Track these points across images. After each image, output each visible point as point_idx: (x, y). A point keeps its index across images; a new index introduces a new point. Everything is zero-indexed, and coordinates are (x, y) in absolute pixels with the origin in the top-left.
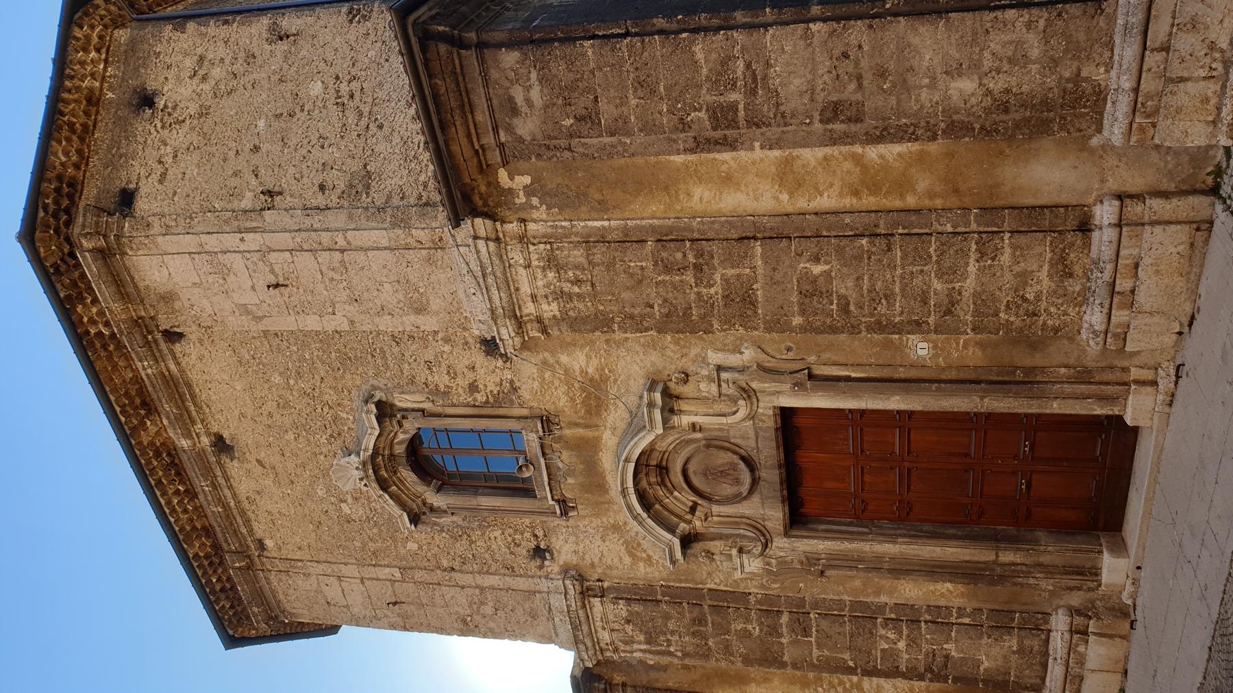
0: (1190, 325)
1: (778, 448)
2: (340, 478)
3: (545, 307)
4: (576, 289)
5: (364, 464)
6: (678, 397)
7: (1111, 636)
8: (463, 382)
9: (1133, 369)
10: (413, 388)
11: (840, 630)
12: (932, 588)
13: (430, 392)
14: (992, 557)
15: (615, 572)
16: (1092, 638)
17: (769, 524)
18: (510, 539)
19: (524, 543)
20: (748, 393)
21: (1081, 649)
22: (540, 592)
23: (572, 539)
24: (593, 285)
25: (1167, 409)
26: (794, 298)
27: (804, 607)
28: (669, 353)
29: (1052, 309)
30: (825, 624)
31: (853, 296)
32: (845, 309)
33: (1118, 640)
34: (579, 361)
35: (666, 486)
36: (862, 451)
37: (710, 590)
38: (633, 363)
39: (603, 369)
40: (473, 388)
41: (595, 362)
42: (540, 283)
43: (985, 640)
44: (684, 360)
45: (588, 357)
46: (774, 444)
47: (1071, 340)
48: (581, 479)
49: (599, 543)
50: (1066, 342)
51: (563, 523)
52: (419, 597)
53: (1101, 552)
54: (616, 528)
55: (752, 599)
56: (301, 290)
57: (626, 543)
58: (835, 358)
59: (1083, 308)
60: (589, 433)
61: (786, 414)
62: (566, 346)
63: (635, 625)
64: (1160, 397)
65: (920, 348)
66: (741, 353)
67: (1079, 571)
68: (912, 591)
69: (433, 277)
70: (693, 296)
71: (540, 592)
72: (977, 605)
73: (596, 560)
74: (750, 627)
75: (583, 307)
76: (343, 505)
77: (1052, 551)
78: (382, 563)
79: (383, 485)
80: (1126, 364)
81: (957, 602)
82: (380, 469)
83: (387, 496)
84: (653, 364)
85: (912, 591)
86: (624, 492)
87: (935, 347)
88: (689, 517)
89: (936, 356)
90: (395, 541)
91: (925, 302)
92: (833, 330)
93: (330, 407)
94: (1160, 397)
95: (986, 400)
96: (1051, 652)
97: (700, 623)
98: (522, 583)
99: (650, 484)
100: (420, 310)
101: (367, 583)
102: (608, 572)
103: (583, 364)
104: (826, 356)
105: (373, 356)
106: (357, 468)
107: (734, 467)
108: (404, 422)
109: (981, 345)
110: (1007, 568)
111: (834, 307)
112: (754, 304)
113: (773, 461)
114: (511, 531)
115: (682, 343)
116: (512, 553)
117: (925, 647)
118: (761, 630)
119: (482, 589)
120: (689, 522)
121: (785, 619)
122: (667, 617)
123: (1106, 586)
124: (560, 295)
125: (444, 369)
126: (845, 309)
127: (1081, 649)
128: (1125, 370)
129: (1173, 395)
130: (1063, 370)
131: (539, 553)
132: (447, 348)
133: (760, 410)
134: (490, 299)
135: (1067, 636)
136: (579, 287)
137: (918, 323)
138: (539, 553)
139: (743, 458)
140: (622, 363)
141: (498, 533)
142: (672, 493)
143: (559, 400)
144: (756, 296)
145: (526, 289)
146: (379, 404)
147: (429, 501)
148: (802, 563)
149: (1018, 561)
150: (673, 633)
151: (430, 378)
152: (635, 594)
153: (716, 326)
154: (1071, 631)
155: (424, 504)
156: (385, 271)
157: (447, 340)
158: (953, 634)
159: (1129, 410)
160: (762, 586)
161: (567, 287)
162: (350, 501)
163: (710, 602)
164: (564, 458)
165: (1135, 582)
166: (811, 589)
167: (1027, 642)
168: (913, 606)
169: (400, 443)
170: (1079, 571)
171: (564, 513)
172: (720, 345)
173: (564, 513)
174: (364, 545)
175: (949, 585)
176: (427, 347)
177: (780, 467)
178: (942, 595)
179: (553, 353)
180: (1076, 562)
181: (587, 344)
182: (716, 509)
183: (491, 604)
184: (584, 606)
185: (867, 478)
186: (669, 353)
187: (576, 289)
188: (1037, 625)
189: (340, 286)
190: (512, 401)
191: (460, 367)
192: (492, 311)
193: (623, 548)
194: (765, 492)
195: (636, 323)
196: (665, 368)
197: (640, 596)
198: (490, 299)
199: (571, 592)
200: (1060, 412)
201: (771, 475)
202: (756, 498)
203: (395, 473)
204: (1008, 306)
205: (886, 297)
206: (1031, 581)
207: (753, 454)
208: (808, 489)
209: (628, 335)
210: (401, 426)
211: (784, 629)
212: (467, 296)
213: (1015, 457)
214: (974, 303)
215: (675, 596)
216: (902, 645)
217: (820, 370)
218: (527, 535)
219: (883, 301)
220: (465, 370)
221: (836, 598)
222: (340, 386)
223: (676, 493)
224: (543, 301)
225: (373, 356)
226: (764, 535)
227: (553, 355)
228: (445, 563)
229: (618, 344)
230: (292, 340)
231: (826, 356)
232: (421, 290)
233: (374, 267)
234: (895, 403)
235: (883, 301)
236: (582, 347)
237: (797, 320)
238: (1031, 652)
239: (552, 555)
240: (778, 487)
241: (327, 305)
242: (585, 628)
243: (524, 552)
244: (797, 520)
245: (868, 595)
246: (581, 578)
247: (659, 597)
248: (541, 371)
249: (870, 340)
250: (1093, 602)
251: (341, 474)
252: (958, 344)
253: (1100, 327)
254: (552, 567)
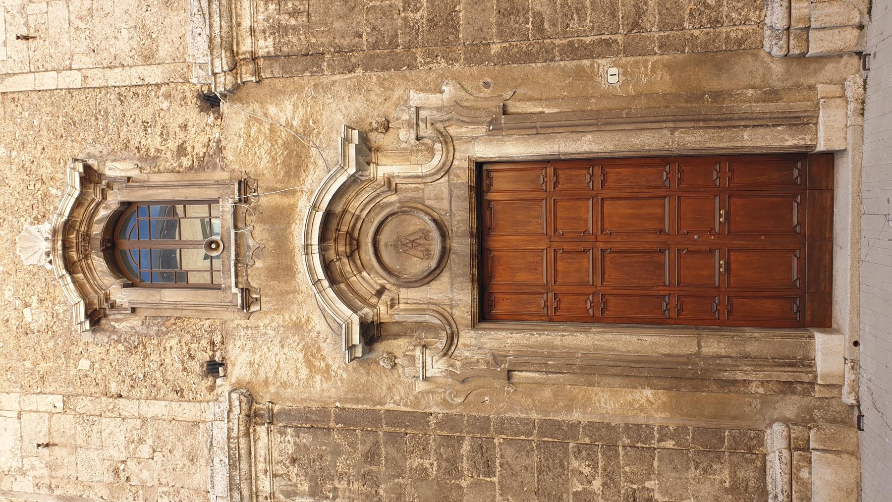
0: (869, 12)
1: (471, 210)
2: (26, 249)
3: (261, 43)
4: (293, 22)
5: (55, 232)
6: (377, 150)
7: (837, 453)
8: (173, 144)
9: (819, 86)
10: (125, 154)
11: (527, 462)
12: (629, 398)
13: (141, 159)
14: (694, 349)
15: (289, 392)
16: (815, 455)
17: (457, 312)
18: (185, 349)
19: (199, 355)
20: (446, 140)
21: (804, 474)
22: (204, 422)
23: (250, 344)
24: (309, 16)
25: (859, 119)
26: (493, 19)
27: (488, 430)
28: (373, 97)
29: (734, 15)
30: (510, 452)
31: (547, 12)
32: (539, 28)
33: (846, 456)
34: (285, 112)
35: (354, 262)
36: (555, 230)
37: (388, 411)
38: (335, 108)
39: (307, 121)
40: (181, 150)
41: (301, 112)
42: (261, 17)
43: (693, 473)
44: (387, 104)
45: (295, 106)
46: (466, 204)
47: (755, 56)
48: (270, 261)
49: (277, 349)
50: (749, 58)
51: (243, 323)
52: (74, 437)
53: (813, 337)
54: (298, 327)
55: (432, 421)
56: (47, 43)
57: (306, 348)
58: (530, 93)
59: (763, 13)
60: (286, 201)
61: (480, 169)
62: (277, 94)
63: (301, 466)
64: (851, 106)
65: (610, 74)
66: (441, 93)
67: (791, 363)
68: (609, 403)
69: (168, 21)
70: (400, 22)
71: (204, 422)
72: (681, 422)
73: (271, 375)
74: (427, 463)
75: (296, 42)
76: (27, 311)
77: (760, 342)
78: (47, 391)
79: (70, 266)
80: (812, 81)
81: (659, 418)
82: (70, 242)
83: (69, 278)
84: (357, 111)
85: (609, 403)
86: (307, 246)
87: (625, 73)
88: (374, 300)
89: (625, 83)
90: (67, 358)
91: (614, 15)
92: (529, 57)
93: (43, 183)
94: (851, 106)
95: (677, 134)
96: (769, 487)
97: (372, 462)
98: (187, 411)
99: (337, 254)
100: (149, 59)
101: (24, 416)
102: (282, 391)
103: (289, 115)
104: (521, 91)
105: (97, 119)
106: (47, 239)
107: (425, 234)
108: (109, 192)
109: (669, 67)
110: (710, 361)
111: (530, 26)
112: (455, 28)
113: (464, 228)
114: (188, 337)
115: (386, 85)
116: (185, 369)
117: (625, 486)
118: (439, 467)
119: (144, 420)
120: (373, 306)
121: (466, 447)
122: (337, 452)
123: (824, 377)
124: (278, 30)
125: (158, 130)
126: (539, 28)
127: (804, 474)
128: (812, 88)
129: (863, 102)
130: (750, 92)
131: (213, 368)
132: (165, 105)
133: (456, 163)
134: (211, 26)
135: (786, 453)
136: (296, 19)
137: (608, 43)
138: (213, 368)
139: (435, 221)
140: (326, 113)
141: (173, 342)
142: (360, 273)
143: (261, 162)
144: (459, 18)
145: (246, 23)
146: (87, 168)
147: (112, 298)
148: (488, 363)
149: (723, 352)
150: (341, 477)
151: (143, 142)
152: (307, 420)
153: (419, 59)
154: (789, 448)
155: (107, 299)
156: (126, 17)
157: (168, 96)
158: (656, 463)
159: (821, 134)
160: (445, 403)
161: (284, 19)
162: (35, 304)
163: (386, 428)
164: (257, 235)
165: (855, 365)
166: (498, 404)
167: (741, 474)
168: (609, 424)
169: (100, 221)
170: (791, 363)
171: (246, 305)
172: (421, 84)
173: (246, 305)
174: (36, 364)
175: (648, 393)
176: (148, 105)
177: (472, 235)
178: (642, 409)
179: (262, 104)
180: (787, 351)
181: (295, 90)
182: (405, 294)
183: (150, 442)
184: (247, 434)
185: (561, 266)
186: (373, 97)
187: (293, 22)
188: (750, 447)
189: (83, 36)
190: (215, 164)
191: (174, 127)
192: (211, 40)
193: (301, 355)
194: (455, 268)
195: (345, 59)
196: (367, 115)
197: (311, 420)
198: (211, 26)
199: (236, 411)
200: (751, 144)
201: (462, 246)
202: (445, 278)
203: (86, 257)
204: (691, 14)
205: (578, 11)
206: (740, 376)
207: (446, 219)
208: (500, 279)
209: (337, 77)
210: (104, 197)
211: (465, 465)
212: (193, 38)
213: (711, 231)
214: (660, 13)
215: (348, 420)
216: (597, 484)
217: (516, 107)
218: (204, 342)
219: (575, 16)
220: (178, 130)
221: (524, 416)
222: (58, 157)
223: (365, 274)
224: (260, 36)
225: (97, 119)
226: (450, 325)
227: (262, 107)
228: (114, 388)
229: (327, 88)
230: (27, 104)
231: (521, 91)
232: (154, 36)
233: (117, 14)
234: (587, 144)
235: (575, 16)
236: (291, 94)
237: (495, 49)
238: (746, 489)
239: (225, 370)
240: (468, 259)
241: (67, 57)
242: (244, 466)
243: (197, 368)
244: (485, 313)
245: (559, 411)
246: (251, 399)
247: (332, 424)
248: (248, 125)
249: (563, 69)
250: (810, 411)
251: (29, 244)
252: (646, 67)
253: (781, 24)
254: (223, 385)
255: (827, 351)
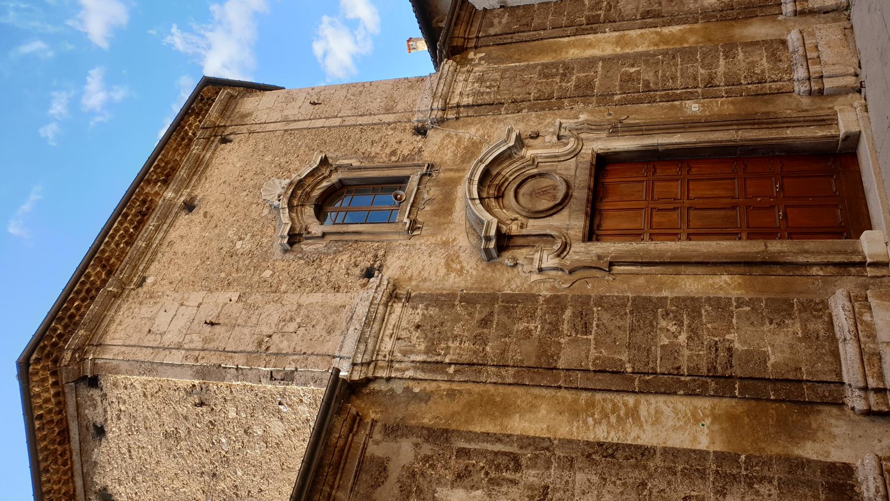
1: (590, 175)
5: (291, 184)
12: (711, 281)
14: (762, 248)
17: (571, 232)
18: (353, 260)
21: (867, 317)
25: (865, 114)
26: (617, 83)
27: (588, 304)
30: (606, 317)
40: (393, 153)
42: (468, 89)
43: (767, 327)
45: (478, 130)
55: (541, 300)
62: (466, 125)
65: (694, 108)
74: (532, 326)
80: (830, 105)
81: (735, 294)
85: (692, 284)
86: (470, 180)
89: (704, 111)
91: (695, 79)
92: (640, 101)
100: (388, 111)
109: (732, 103)
117: (707, 339)
118: (542, 329)
121: (568, 313)
122: (457, 319)
127: (867, 317)
131: (369, 274)
135: (848, 304)
150: (455, 337)
158: (734, 321)
167: (811, 326)
175: (726, 277)
177: (589, 189)
178: (721, 288)
188: (819, 309)
193: (443, 261)
194: (573, 207)
197: (442, 300)
202: (565, 212)
203: (302, 205)
205: (672, 78)
207: (572, 183)
210: (330, 175)
216: (682, 338)
234: (677, 139)
238: (817, 338)
242: (376, 326)
255: (871, 244)
